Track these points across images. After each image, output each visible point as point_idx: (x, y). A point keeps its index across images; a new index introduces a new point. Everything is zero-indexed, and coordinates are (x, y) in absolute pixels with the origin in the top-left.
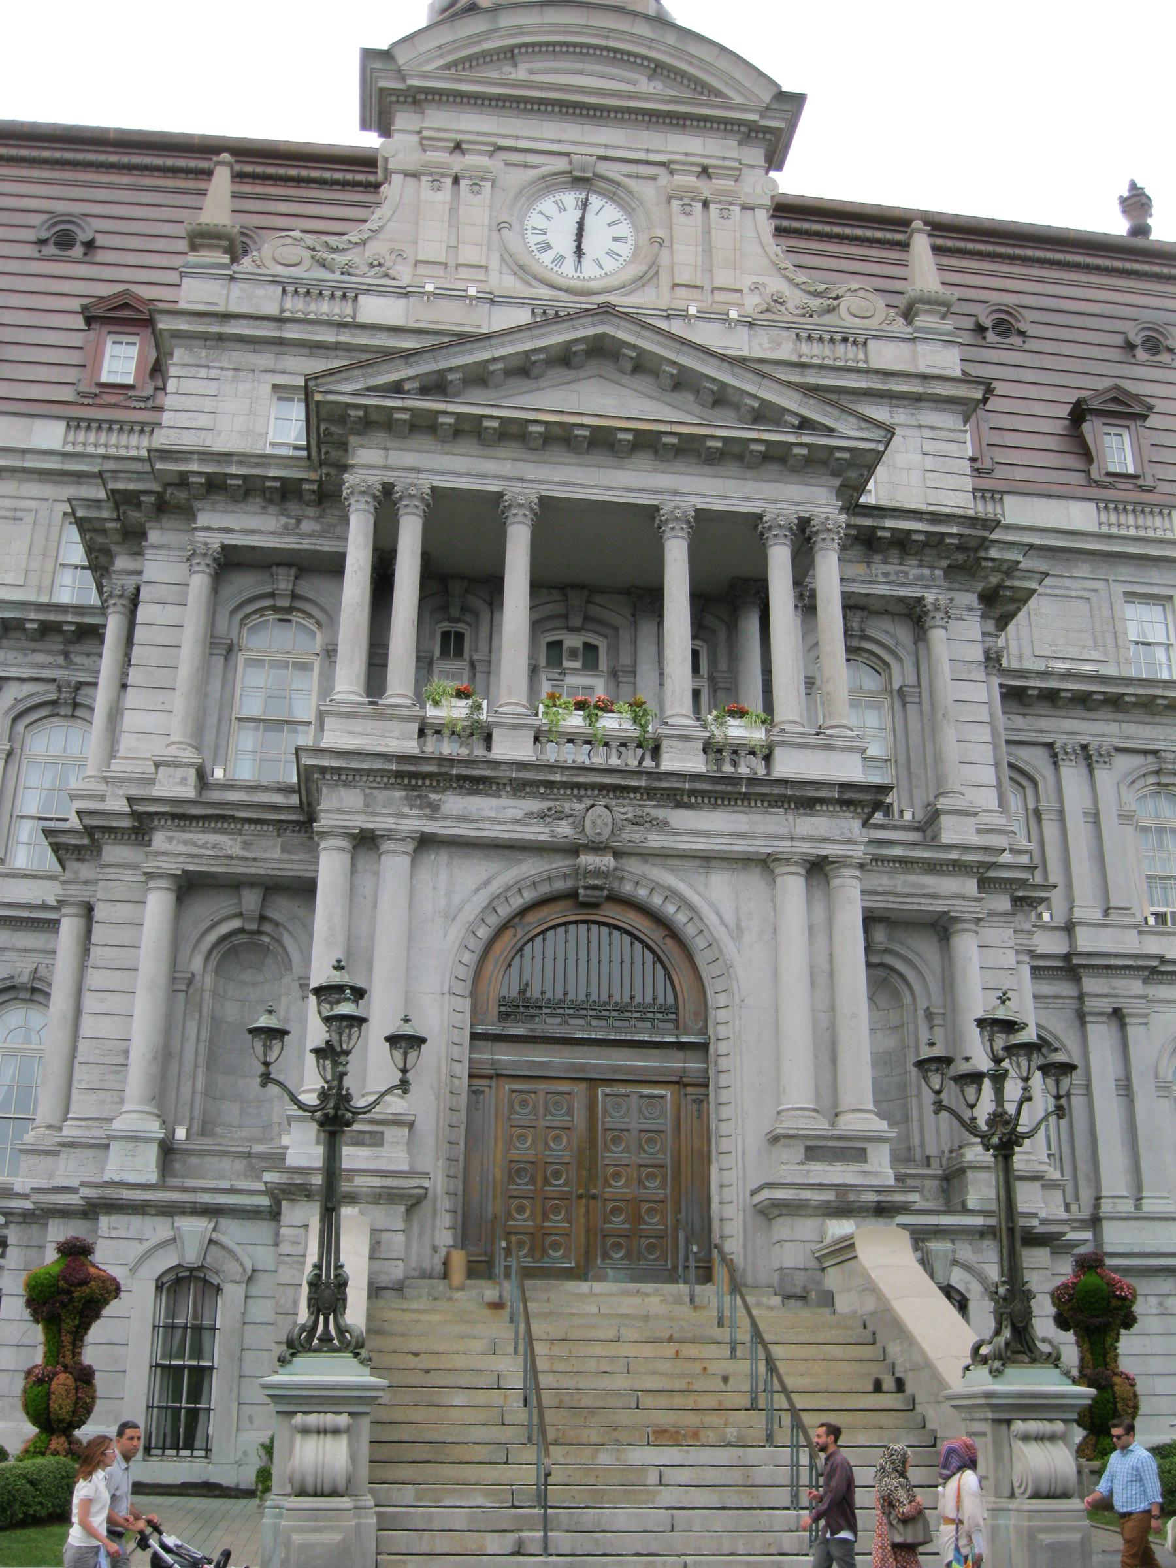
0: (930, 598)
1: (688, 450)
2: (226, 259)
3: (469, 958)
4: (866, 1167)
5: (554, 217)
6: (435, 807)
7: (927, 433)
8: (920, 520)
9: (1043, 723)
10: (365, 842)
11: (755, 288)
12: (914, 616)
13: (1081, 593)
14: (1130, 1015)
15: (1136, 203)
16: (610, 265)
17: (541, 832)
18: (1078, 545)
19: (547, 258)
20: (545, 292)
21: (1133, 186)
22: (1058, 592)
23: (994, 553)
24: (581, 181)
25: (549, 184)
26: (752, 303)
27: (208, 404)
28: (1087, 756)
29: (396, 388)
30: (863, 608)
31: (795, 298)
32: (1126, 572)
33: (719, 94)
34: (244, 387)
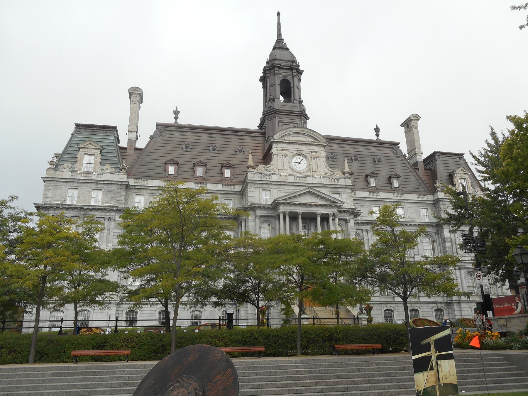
0: (348, 218)
1: (321, 206)
2: (253, 170)
9: (361, 226)
11: (324, 171)
12: (346, 221)
15: (377, 130)
16: (304, 168)
19: (295, 167)
20: (296, 173)
21: (377, 126)
24: (299, 155)
25: (295, 155)
26: (323, 173)
27: (254, 193)
29: (285, 200)
31: (329, 172)
32: (373, 203)
34: (258, 190)
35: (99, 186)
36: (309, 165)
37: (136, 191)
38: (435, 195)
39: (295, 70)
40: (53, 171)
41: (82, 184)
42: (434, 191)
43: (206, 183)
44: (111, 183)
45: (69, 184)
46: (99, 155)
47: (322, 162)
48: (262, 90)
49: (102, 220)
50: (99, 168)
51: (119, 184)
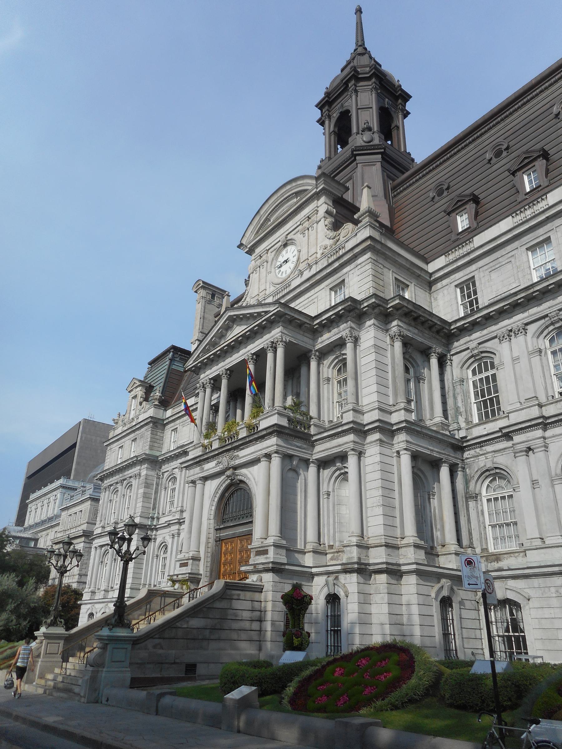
0: (344, 334)
3: (213, 508)
4: (268, 556)
6: (203, 468)
7: (359, 267)
8: (331, 311)
10: (193, 482)
13: (507, 261)
14: (536, 448)
17: (218, 469)
18: (499, 242)
22: (497, 266)
23: (365, 304)
24: (285, 245)
25: (278, 252)
28: (510, 333)
30: (337, 346)
33: (306, 190)
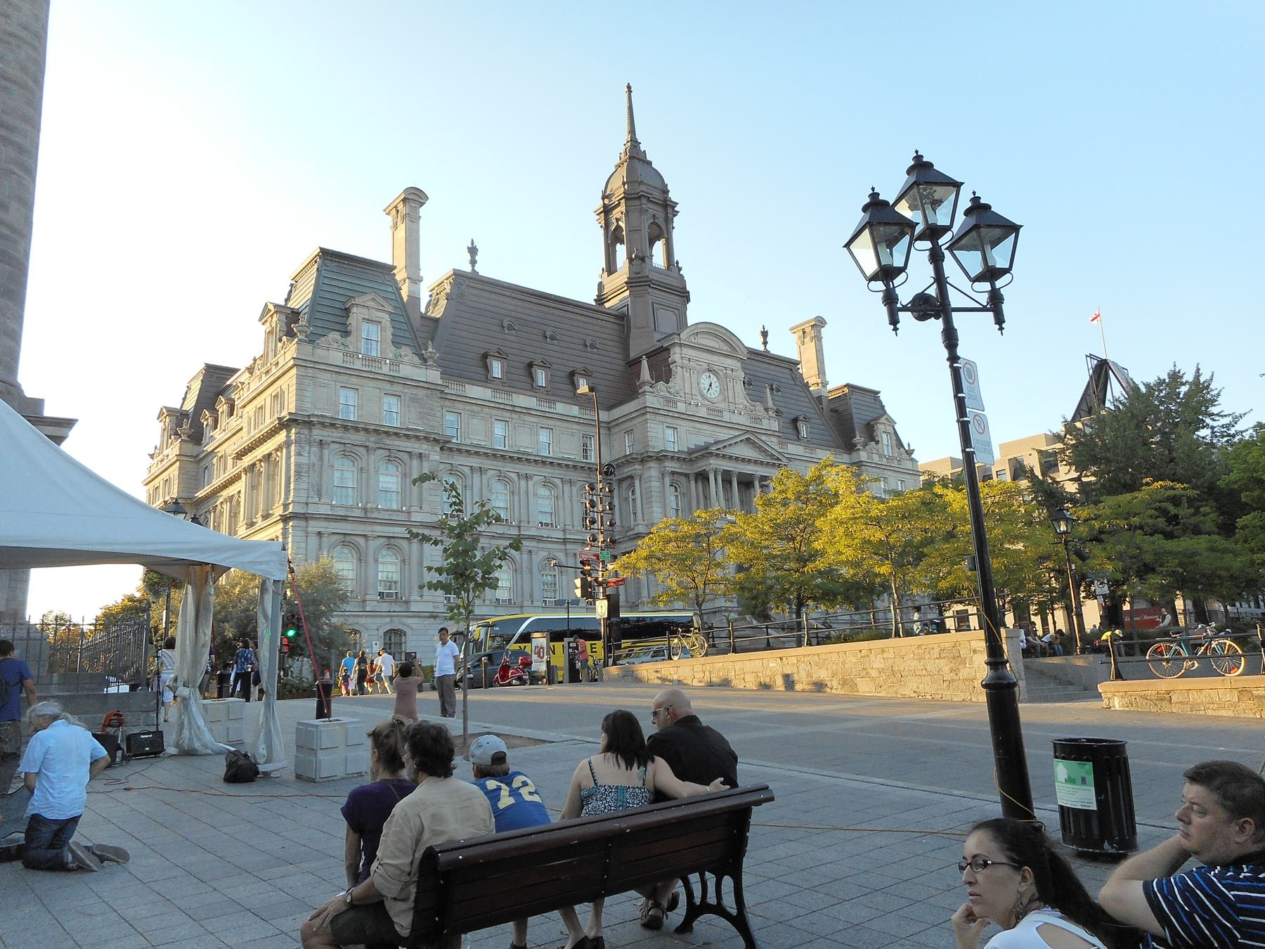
5: (705, 380)
24: (709, 371)
35: (398, 389)
36: (723, 390)
37: (447, 403)
38: (854, 454)
39: (668, 208)
40: (309, 348)
41: (365, 381)
42: (850, 447)
43: (554, 402)
44: (418, 385)
45: (341, 377)
46: (388, 324)
47: (739, 387)
48: (601, 232)
49: (405, 457)
50: (391, 351)
51: (429, 387)
